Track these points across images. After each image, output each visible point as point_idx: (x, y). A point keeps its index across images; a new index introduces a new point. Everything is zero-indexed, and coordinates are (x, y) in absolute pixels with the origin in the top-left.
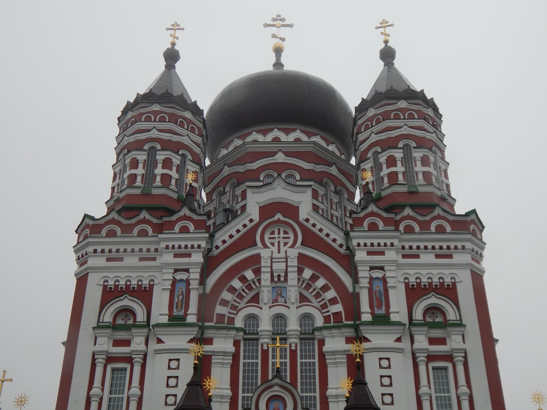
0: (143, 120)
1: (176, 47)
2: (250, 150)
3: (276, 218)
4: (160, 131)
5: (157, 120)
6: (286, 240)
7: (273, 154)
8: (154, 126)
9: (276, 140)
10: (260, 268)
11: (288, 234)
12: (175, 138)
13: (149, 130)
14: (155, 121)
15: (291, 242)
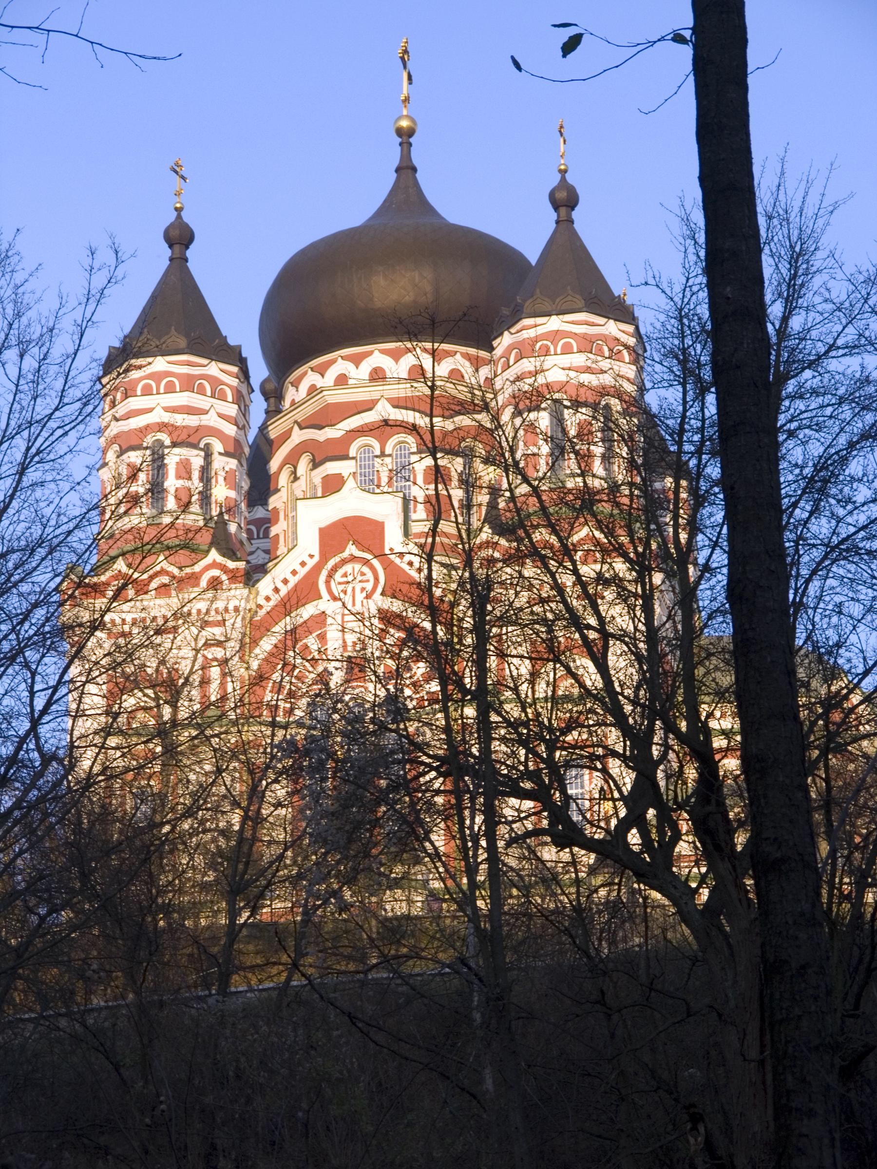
0: (139, 393)
1: (186, 217)
2: (331, 400)
3: (346, 554)
4: (167, 409)
5: (162, 391)
6: (364, 585)
7: (368, 406)
8: (157, 402)
9: (378, 376)
10: (325, 631)
11: (365, 574)
12: (192, 421)
13: (150, 410)
14: (158, 393)
15: (369, 586)
